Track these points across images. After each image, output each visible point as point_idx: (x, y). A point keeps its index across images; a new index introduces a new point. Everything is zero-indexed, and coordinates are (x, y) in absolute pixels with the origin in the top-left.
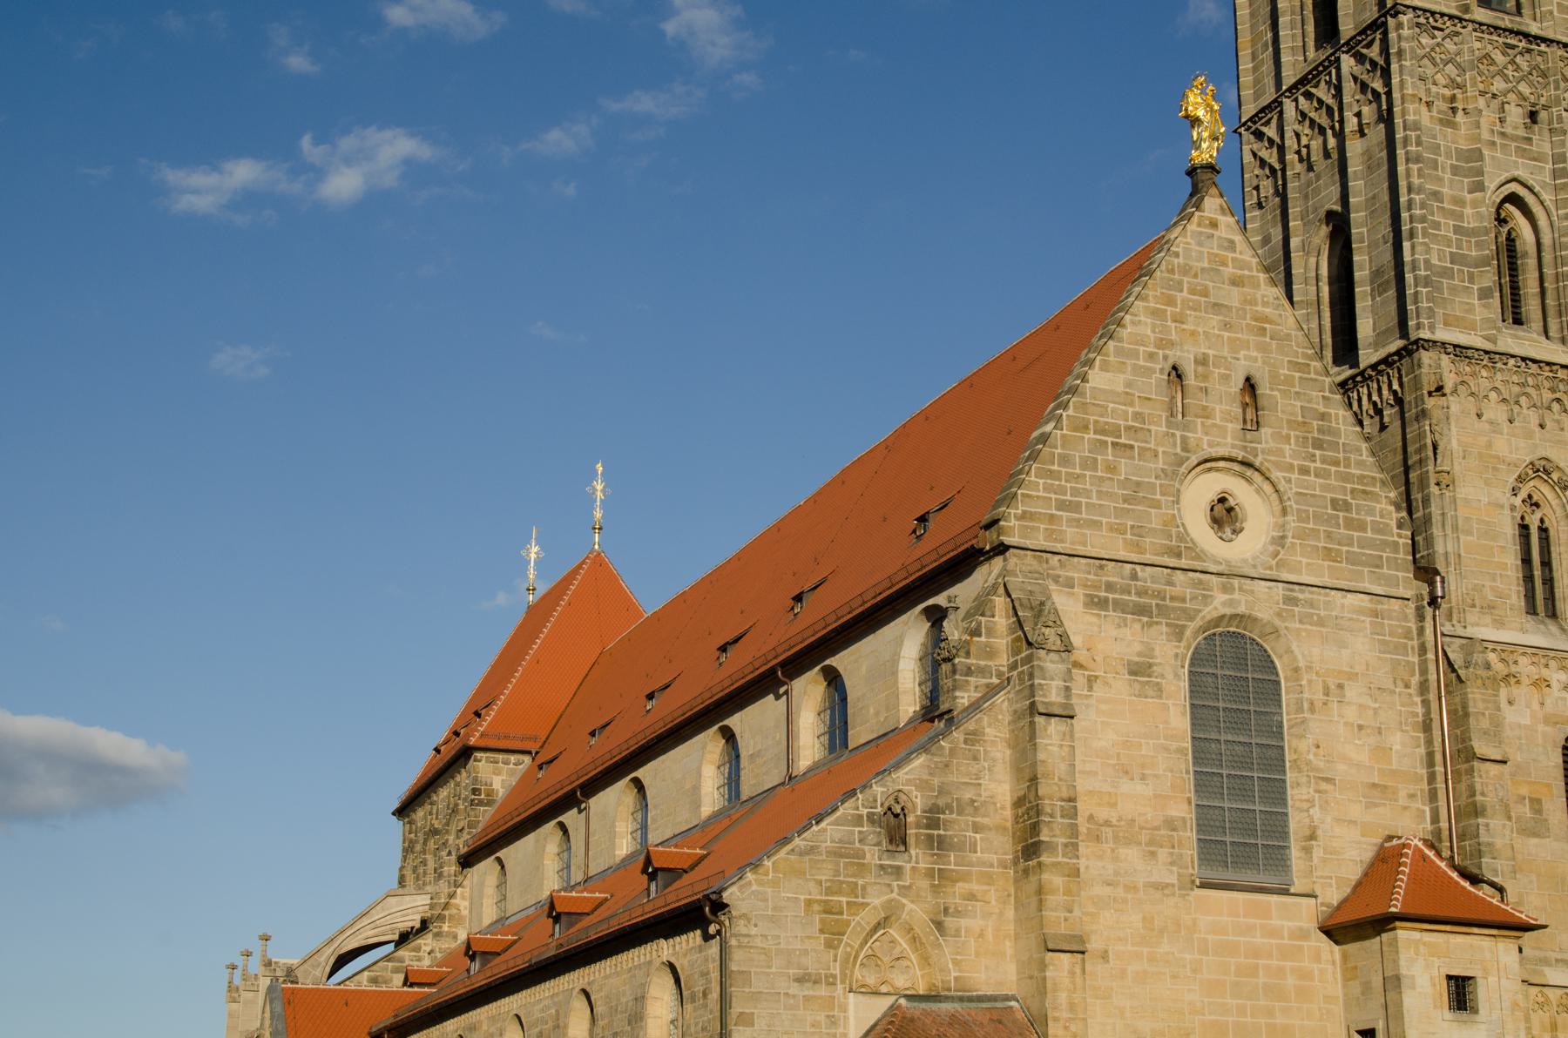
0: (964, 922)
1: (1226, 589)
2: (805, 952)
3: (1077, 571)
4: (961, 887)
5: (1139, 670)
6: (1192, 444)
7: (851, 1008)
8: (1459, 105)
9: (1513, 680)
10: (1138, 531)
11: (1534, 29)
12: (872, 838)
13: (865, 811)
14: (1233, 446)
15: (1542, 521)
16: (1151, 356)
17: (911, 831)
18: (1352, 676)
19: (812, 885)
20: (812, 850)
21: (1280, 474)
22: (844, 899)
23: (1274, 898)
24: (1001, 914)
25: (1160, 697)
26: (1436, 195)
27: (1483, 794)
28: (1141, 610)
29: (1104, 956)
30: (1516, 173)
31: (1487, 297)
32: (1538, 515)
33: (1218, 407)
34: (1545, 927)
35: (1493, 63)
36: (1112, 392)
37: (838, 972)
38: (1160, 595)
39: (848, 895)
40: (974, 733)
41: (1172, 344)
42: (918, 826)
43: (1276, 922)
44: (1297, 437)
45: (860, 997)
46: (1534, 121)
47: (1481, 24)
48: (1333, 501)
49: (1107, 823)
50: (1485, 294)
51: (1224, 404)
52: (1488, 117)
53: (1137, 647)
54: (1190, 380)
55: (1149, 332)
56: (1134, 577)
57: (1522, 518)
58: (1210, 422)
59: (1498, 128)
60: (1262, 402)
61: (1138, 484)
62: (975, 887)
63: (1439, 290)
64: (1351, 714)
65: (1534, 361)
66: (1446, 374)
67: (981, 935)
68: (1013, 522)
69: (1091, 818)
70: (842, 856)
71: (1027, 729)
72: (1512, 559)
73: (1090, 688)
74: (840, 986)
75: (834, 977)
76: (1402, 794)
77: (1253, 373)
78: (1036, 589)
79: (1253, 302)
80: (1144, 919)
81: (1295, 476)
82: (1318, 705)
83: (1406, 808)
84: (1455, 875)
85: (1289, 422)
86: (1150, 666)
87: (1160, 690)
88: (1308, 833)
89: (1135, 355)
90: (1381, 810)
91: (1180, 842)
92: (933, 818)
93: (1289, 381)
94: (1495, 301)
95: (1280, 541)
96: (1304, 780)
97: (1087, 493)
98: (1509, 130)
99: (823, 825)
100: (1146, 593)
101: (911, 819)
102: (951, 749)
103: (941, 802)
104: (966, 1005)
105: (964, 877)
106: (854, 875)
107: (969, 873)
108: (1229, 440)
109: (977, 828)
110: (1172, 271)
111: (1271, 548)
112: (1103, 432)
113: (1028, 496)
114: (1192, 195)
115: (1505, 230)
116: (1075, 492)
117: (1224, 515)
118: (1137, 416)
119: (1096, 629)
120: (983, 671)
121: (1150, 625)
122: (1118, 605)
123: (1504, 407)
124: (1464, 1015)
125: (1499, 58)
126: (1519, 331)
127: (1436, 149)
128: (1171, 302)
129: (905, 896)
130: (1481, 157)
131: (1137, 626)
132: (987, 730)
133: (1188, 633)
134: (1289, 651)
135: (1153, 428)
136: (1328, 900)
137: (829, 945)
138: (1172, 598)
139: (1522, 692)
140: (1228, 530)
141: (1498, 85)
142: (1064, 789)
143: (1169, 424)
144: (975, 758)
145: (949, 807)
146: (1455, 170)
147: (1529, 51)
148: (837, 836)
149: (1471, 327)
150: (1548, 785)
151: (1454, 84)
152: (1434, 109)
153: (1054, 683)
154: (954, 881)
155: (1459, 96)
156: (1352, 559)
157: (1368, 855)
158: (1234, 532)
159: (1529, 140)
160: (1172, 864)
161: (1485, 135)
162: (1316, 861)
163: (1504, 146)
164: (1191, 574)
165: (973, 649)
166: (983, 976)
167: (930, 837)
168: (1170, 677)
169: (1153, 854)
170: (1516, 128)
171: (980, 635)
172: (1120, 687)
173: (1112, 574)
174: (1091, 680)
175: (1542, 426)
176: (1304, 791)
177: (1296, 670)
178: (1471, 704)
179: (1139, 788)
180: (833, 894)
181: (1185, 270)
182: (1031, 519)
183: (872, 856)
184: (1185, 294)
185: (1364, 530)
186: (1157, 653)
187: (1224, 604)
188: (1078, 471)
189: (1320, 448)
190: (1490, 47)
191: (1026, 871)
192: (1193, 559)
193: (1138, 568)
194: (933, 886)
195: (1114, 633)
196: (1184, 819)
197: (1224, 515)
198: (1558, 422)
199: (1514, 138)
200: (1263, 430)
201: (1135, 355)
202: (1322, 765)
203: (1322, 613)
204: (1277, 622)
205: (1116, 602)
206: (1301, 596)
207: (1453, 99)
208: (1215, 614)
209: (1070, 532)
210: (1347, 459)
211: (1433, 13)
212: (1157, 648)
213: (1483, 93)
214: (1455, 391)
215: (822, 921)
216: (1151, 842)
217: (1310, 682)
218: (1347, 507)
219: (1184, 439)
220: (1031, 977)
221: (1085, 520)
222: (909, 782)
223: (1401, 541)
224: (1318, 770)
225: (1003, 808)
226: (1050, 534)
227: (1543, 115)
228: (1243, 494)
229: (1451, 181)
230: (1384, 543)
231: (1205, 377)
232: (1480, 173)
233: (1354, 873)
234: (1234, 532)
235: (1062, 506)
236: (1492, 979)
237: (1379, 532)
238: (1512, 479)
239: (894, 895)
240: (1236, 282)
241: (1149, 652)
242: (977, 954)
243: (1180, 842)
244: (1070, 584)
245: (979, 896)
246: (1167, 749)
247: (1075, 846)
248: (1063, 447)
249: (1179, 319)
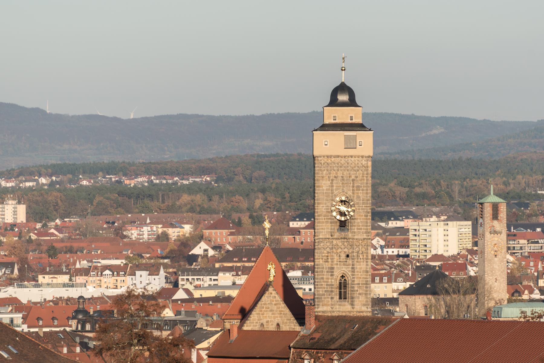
8: (329, 257)
16: (257, 323)
26: (323, 278)
41: (261, 319)
79: (279, 308)
89: (253, 323)
93: (286, 323)
98: (341, 260)
127: (323, 268)
128: (261, 311)
130: (333, 268)
146: (327, 272)
151: (328, 253)
161: (335, 262)
181: (265, 304)
201: (253, 323)
207: (328, 256)
227: (350, 255)
232: (333, 272)
240: (275, 305)
249: (263, 314)
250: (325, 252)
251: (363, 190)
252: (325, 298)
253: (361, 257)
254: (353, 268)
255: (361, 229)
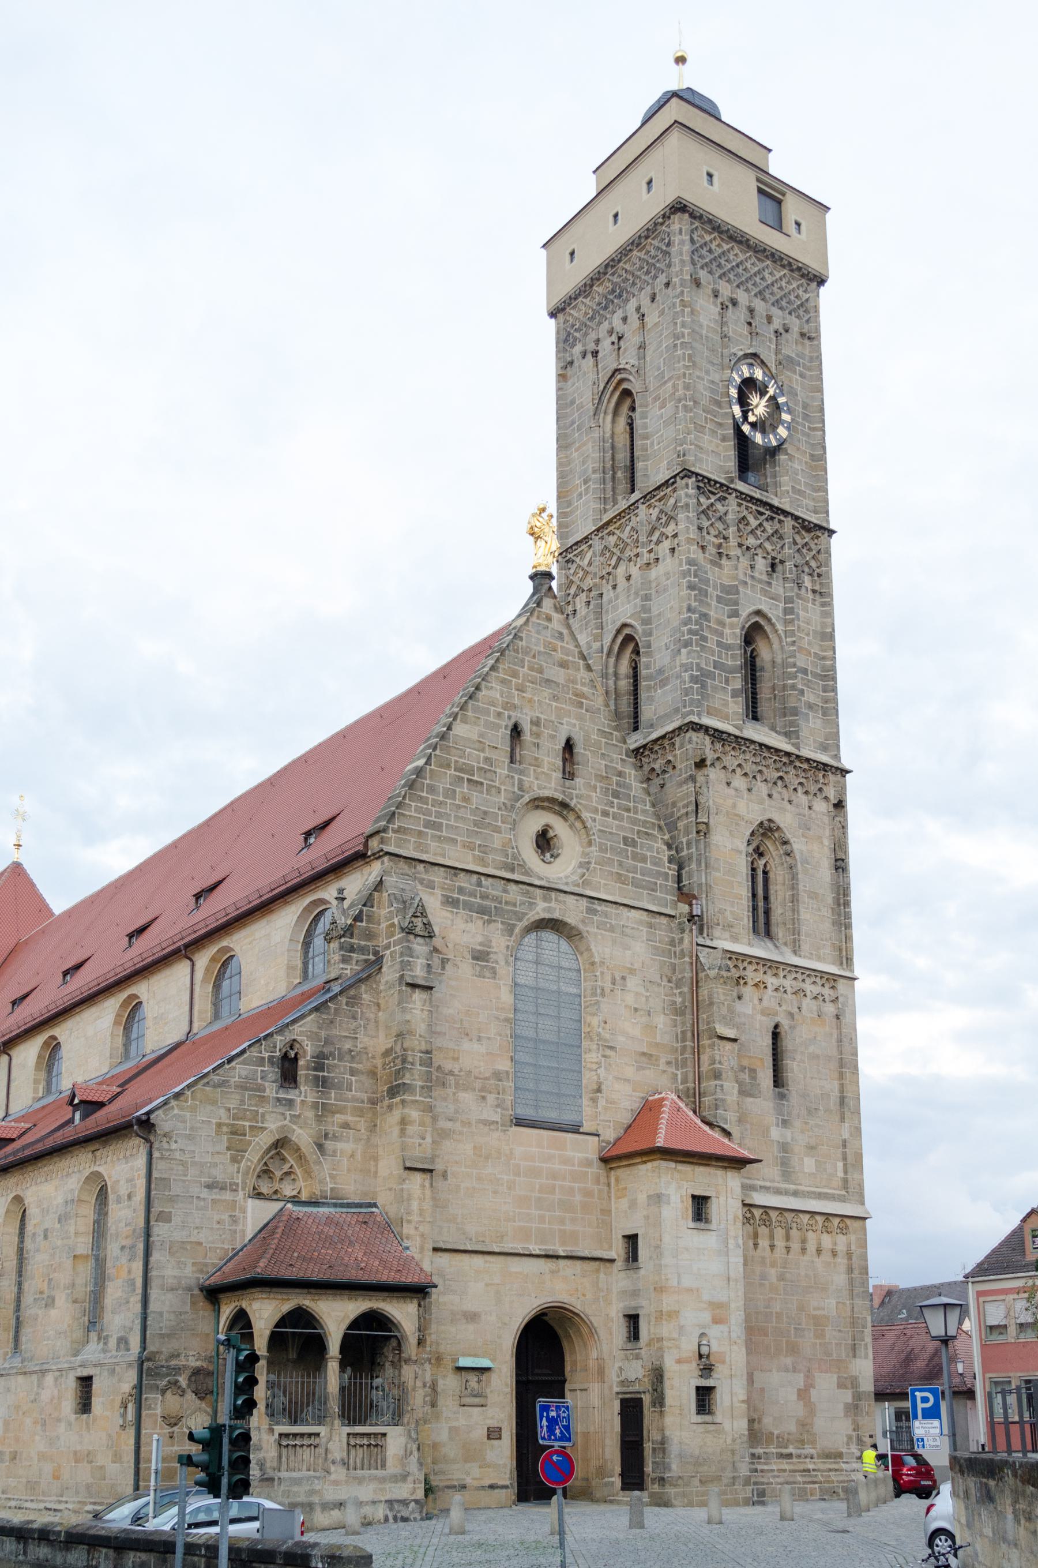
0: (340, 1145)
1: (546, 899)
2: (215, 1165)
3: (437, 876)
4: (339, 1118)
5: (480, 956)
6: (526, 785)
7: (249, 1210)
9: (742, 982)
10: (484, 849)
11: (775, 502)
12: (271, 1076)
13: (268, 1054)
14: (556, 790)
15: (765, 866)
16: (499, 715)
17: (301, 1072)
18: (632, 971)
19: (222, 1112)
20: (223, 1084)
21: (588, 815)
22: (247, 1124)
23: (570, 1135)
24: (368, 1139)
25: (494, 978)
26: (705, 616)
27: (720, 1063)
28: (483, 911)
29: (444, 1175)
30: (760, 607)
31: (737, 696)
32: (762, 862)
33: (546, 759)
34: (760, 1161)
35: (747, 524)
36: (469, 739)
37: (240, 1181)
38: (496, 899)
39: (250, 1120)
40: (354, 997)
42: (308, 1069)
43: (569, 1153)
44: (602, 788)
45: (257, 1202)
46: (773, 571)
47: (742, 493)
48: (625, 839)
49: (451, 1073)
50: (735, 694)
51: (551, 758)
52: (744, 562)
53: (480, 939)
54: (527, 737)
55: (498, 696)
56: (479, 884)
57: (752, 863)
58: (540, 770)
59: (749, 572)
60: (577, 758)
61: (485, 813)
62: (349, 1118)
63: (704, 686)
64: (630, 999)
65: (767, 746)
66: (707, 751)
67: (352, 1156)
68: (390, 834)
69: (439, 1067)
70: (246, 1089)
71: (396, 995)
72: (745, 892)
73: (443, 968)
74: (241, 1193)
75: (237, 1185)
76: (663, 1061)
77: (573, 735)
78: (407, 888)
80: (475, 1147)
81: (598, 817)
82: (607, 991)
83: (664, 1071)
84: (698, 1122)
85: (596, 775)
86: (488, 953)
87: (495, 973)
88: (595, 1087)
90: (647, 1072)
91: (504, 1090)
92: (320, 1062)
94: (741, 700)
95: (585, 865)
96: (595, 1047)
97: (448, 816)
98: (756, 575)
99: (233, 1064)
100: (487, 897)
101: (301, 1062)
102: (335, 1009)
103: (326, 1050)
104: (338, 1210)
105: (341, 1111)
106: (256, 1106)
107: (345, 1107)
108: (553, 785)
109: (353, 1072)
110: (517, 651)
111: (580, 871)
112: (461, 770)
113: (403, 815)
114: (533, 595)
115: (749, 650)
116: (439, 815)
117: (544, 841)
118: (487, 760)
119: (449, 922)
120: (363, 950)
121: (489, 922)
122: (468, 906)
123: (744, 779)
124: (702, 1225)
125: (754, 523)
126: (757, 725)
127: (707, 581)
128: (515, 674)
129: (295, 1123)
130: (737, 593)
131: (480, 923)
132: (364, 996)
133: (517, 930)
134: (589, 949)
135: (498, 771)
136: (607, 1138)
137: (234, 1160)
138: (506, 903)
139: (748, 991)
140: (548, 855)
141: (751, 541)
142: (423, 1043)
143: (510, 769)
144: (354, 1018)
145: (332, 1054)
146: (719, 600)
147: (772, 518)
148: (244, 1073)
149: (726, 718)
150: (762, 1060)
152: (707, 552)
153: (419, 961)
154: (334, 1113)
155: (724, 545)
156: (636, 884)
157: (637, 1105)
158: (552, 856)
159: (769, 584)
160: (497, 1106)
162: (600, 1108)
163: (753, 586)
164: (521, 886)
165: (356, 932)
166: (352, 1188)
167: (317, 1077)
168: (502, 963)
169: (484, 1098)
170: (761, 574)
171: (362, 921)
172: (465, 969)
173: (464, 882)
174: (444, 962)
175: (770, 796)
176: (594, 1055)
177: (593, 964)
178: (715, 996)
179: (476, 1046)
180: (238, 1119)
182: (404, 833)
183: (271, 1090)
184: (526, 669)
185: (645, 862)
186: (494, 944)
187: (544, 910)
188: (441, 799)
189: (618, 797)
190: (745, 513)
191: (390, 1107)
192: (523, 874)
193: (483, 878)
194: (317, 1116)
195: (463, 926)
196: (507, 1072)
197: (544, 841)
198: (780, 793)
199: (760, 581)
200: (577, 780)
202: (607, 1036)
203: (613, 922)
204: (581, 927)
205: (465, 902)
206: (599, 908)
208: (537, 917)
209: (433, 845)
210: (635, 807)
211: (709, 480)
212: (494, 940)
213: (740, 545)
214: (713, 765)
215: (229, 1139)
216: (482, 1090)
217: (602, 973)
218: (634, 844)
219: (520, 781)
220: (390, 1189)
221: (445, 838)
222: (301, 1033)
223: (671, 872)
224: (606, 1040)
225: (373, 1057)
226: (418, 847)
228: (560, 828)
229: (716, 607)
230: (658, 872)
231: (538, 735)
233: (626, 1118)
234: (552, 856)
235: (428, 824)
236: (722, 1199)
237: (655, 864)
238: (748, 833)
239: (286, 1122)
240: (563, 665)
241: (487, 943)
242: (349, 1170)
243: (504, 1090)
244: (431, 886)
245: (352, 1125)
246: (497, 1018)
247: (430, 1088)
248: (431, 778)
249: (521, 689)
250: (713, 532)
251: (802, 375)
252: (715, 688)
253: (807, 581)
254: (787, 611)
255: (800, 492)
